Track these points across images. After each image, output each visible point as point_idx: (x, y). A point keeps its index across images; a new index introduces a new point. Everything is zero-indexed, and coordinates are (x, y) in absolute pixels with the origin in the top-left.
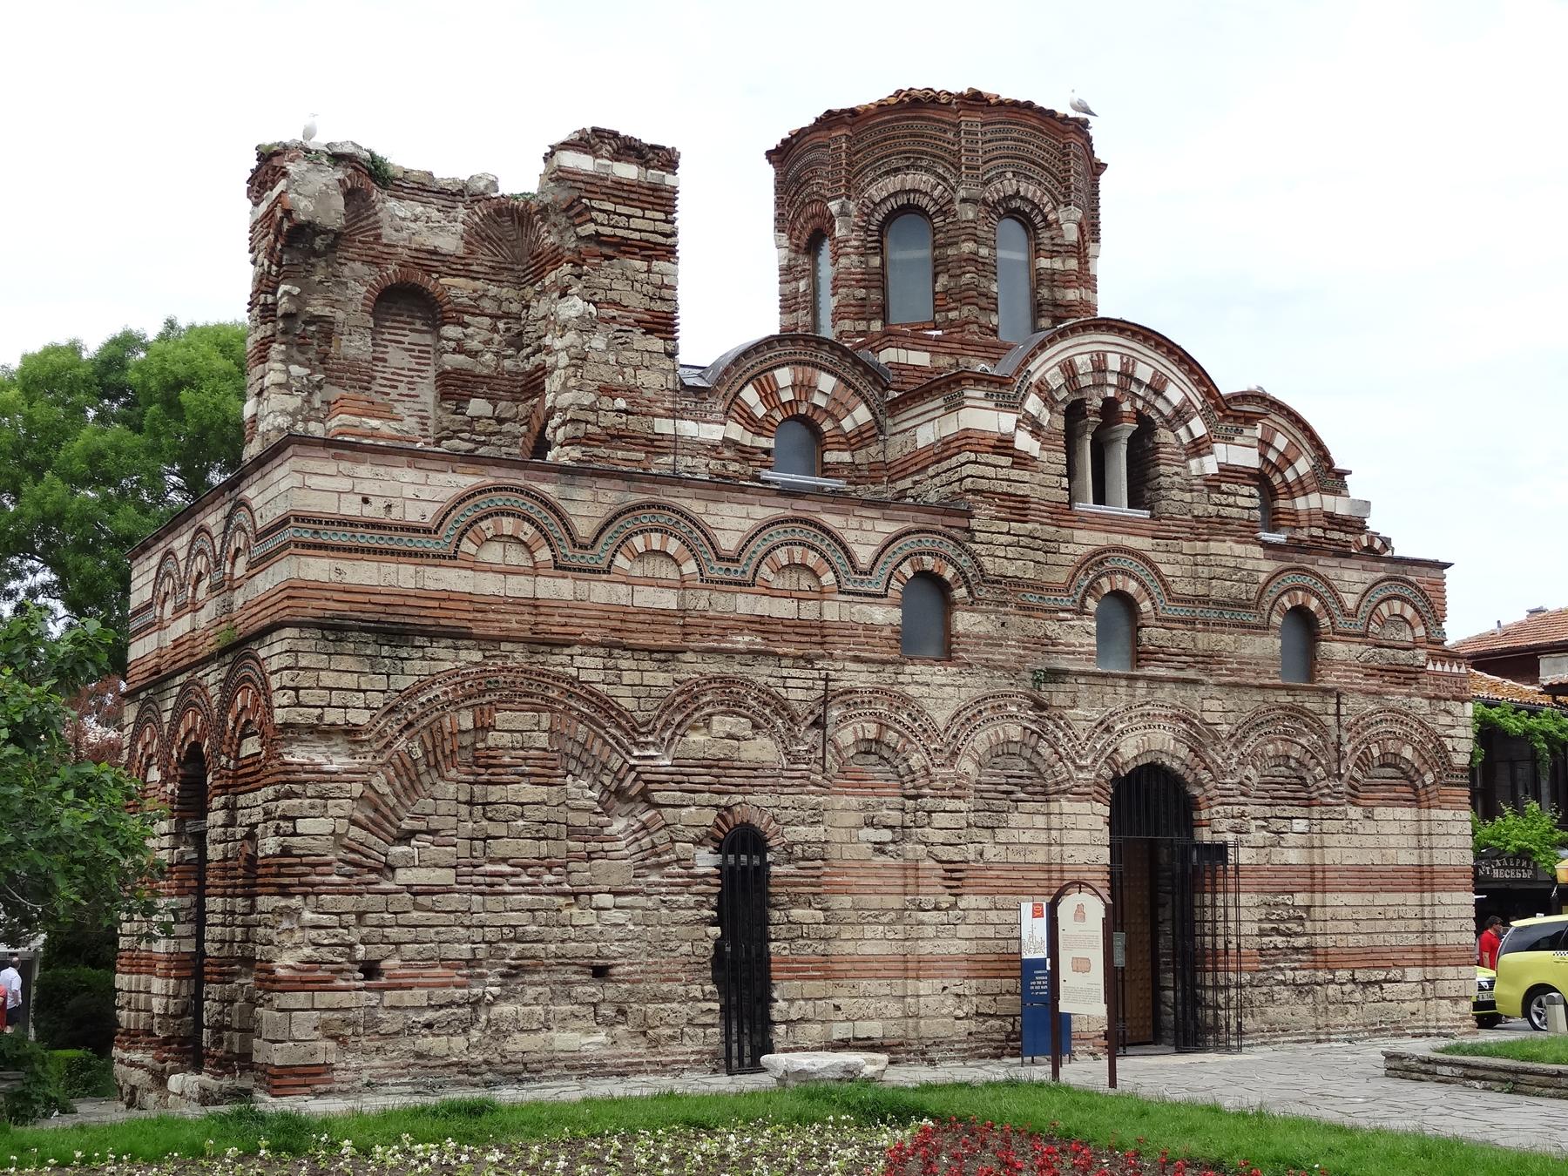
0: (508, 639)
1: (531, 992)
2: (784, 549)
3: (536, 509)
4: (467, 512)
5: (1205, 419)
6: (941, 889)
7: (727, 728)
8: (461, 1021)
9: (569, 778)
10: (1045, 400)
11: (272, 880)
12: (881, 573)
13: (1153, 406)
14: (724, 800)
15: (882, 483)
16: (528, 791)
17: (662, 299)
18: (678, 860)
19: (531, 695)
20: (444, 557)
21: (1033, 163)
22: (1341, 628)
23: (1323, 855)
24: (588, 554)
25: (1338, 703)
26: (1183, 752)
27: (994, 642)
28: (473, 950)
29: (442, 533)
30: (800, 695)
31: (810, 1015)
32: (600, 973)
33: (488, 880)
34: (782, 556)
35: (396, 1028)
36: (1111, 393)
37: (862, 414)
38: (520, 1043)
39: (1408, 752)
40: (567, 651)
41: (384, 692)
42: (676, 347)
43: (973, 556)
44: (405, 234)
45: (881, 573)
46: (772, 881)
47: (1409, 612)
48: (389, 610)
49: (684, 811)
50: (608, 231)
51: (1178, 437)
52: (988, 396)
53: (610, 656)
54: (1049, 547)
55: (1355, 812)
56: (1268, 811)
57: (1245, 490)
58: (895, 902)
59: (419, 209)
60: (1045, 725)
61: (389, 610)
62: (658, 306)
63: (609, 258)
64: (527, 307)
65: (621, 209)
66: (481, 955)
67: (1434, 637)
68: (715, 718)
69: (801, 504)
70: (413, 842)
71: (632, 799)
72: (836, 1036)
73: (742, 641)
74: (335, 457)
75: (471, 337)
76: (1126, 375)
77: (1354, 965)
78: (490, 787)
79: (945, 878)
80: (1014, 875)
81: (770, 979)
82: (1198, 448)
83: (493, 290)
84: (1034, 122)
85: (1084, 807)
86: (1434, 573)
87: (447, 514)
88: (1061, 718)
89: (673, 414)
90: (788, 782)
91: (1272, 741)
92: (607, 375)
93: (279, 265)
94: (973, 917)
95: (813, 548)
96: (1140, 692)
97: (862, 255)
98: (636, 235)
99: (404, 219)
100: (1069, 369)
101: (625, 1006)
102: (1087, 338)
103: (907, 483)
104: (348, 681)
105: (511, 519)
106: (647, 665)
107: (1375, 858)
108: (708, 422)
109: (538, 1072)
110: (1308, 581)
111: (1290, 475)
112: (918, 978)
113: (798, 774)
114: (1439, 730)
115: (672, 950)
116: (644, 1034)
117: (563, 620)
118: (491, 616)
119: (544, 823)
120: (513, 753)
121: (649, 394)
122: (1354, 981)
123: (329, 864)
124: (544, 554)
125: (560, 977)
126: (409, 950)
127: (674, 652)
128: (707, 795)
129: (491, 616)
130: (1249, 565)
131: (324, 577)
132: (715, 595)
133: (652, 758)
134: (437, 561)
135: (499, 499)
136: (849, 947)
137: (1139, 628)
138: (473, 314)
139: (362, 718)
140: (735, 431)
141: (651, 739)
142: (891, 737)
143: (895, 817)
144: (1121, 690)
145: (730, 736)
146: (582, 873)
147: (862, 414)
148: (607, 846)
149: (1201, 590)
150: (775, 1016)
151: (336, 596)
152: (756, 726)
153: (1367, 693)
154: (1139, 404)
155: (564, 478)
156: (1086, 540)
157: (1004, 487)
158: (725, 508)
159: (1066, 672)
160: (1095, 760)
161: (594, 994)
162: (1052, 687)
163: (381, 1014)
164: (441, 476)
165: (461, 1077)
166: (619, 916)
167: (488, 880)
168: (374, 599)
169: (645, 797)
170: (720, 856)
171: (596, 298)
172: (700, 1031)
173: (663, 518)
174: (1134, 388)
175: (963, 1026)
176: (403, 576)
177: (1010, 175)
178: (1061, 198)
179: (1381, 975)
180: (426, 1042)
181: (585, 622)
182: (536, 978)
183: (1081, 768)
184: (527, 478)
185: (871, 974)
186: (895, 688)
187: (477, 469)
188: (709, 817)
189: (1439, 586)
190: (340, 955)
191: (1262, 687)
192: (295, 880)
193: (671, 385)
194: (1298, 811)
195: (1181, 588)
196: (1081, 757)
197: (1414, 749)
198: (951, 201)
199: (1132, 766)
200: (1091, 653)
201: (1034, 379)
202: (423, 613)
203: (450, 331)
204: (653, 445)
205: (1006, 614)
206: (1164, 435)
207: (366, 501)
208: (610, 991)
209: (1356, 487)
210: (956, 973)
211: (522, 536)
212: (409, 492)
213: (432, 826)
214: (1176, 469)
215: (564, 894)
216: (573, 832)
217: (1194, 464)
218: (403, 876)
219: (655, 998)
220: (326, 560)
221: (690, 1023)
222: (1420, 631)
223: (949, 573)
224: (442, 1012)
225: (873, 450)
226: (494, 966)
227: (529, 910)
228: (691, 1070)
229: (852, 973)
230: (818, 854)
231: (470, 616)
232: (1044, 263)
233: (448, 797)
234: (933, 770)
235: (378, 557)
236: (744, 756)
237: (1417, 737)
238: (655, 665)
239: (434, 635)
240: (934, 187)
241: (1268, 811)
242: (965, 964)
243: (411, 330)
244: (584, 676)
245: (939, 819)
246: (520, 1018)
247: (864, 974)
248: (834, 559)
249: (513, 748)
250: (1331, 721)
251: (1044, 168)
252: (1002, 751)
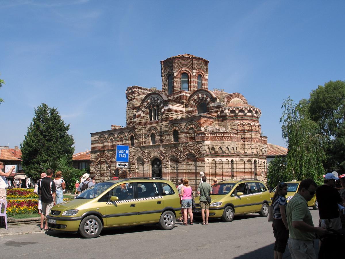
10: (145, 108)
27: (137, 143)
39: (193, 152)
57: (168, 113)
82: (163, 107)
95: (122, 135)
104: (94, 156)
107: (189, 171)
111: (207, 102)
139: (94, 159)
183: (147, 159)
196: (147, 158)
197: (195, 151)
250: (180, 148)
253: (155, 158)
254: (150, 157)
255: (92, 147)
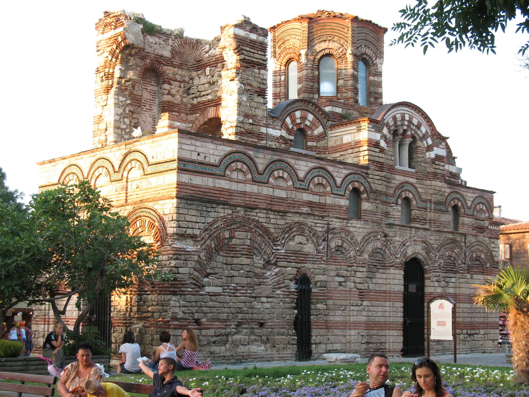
0: (240, 206)
1: (244, 331)
2: (317, 178)
3: (247, 160)
4: (227, 160)
5: (432, 139)
6: (358, 299)
7: (300, 240)
8: (224, 341)
9: (254, 256)
11: (167, 289)
12: (343, 188)
13: (417, 133)
14: (299, 265)
15: (326, 154)
16: (245, 260)
17: (263, 84)
18: (285, 287)
19: (244, 226)
20: (221, 176)
21: (370, 42)
22: (467, 212)
23: (459, 290)
24: (262, 177)
25: (465, 239)
26: (424, 254)
27: (373, 213)
28: (228, 316)
29: (221, 167)
30: (320, 229)
31: (322, 342)
32: (261, 325)
33: (232, 291)
34: (316, 180)
35: (205, 343)
36: (405, 128)
37: (320, 129)
38: (242, 349)
39: (483, 256)
40: (256, 211)
41: (203, 223)
42: (267, 101)
43: (369, 183)
44: (153, 49)
45: (343, 188)
46: (312, 294)
47: (484, 208)
48: (206, 194)
49: (288, 269)
50: (247, 58)
51: (423, 144)
52: (373, 127)
53: (267, 213)
54: (388, 180)
55: (469, 276)
56: (445, 275)
58: (344, 303)
59: (157, 40)
60: (387, 243)
61: (206, 194)
62: (262, 86)
63: (247, 68)
64: (192, 79)
65: (252, 50)
66: (230, 318)
67: (491, 217)
68: (297, 237)
69: (322, 162)
70: (210, 277)
71: (271, 264)
72: (328, 349)
73: (305, 210)
74: (190, 138)
75: (173, 89)
76: (410, 122)
77: (467, 328)
78: (234, 259)
79: (359, 295)
80: (378, 294)
81: (311, 328)
82: (430, 148)
83: (180, 72)
84: (371, 28)
85: (397, 271)
86: (491, 195)
87: (222, 160)
88: (392, 240)
89: (267, 126)
90: (316, 260)
91: (447, 251)
92: (247, 110)
93: (117, 58)
94: (366, 308)
95: (324, 178)
96: (413, 232)
97: (312, 70)
98: (256, 60)
99: (152, 43)
100: (394, 118)
101: (269, 337)
102: (400, 108)
103: (338, 155)
104: (194, 219)
105: (240, 163)
106: (278, 217)
108: (276, 129)
109: (246, 359)
110: (458, 196)
112: (350, 329)
113: (319, 257)
114: (491, 249)
115: (284, 318)
116: (275, 347)
117: (254, 200)
118: (233, 197)
119: (248, 271)
120: (240, 247)
121: (259, 118)
122: (467, 333)
123: (187, 284)
124: (249, 176)
125: (251, 326)
126: (209, 315)
127: (285, 212)
128: (294, 264)
129: (233, 197)
130: (443, 190)
131: (187, 182)
132: (297, 193)
133: (278, 250)
134: (219, 177)
135: (237, 156)
136: (331, 318)
137: (411, 210)
138: (174, 81)
139: (197, 232)
140: (284, 133)
141: (279, 243)
142: (345, 245)
143: (344, 273)
144: (408, 231)
145: (300, 243)
146: (258, 290)
147: (320, 129)
148: (265, 280)
149: (429, 198)
150: (312, 341)
151: (190, 188)
152: (307, 240)
153: (473, 235)
154: (413, 132)
155: (256, 149)
156: (399, 179)
157: (377, 159)
158: (301, 163)
159: (394, 225)
160: (401, 256)
161: (261, 333)
162: (389, 230)
163: (201, 338)
164: (221, 147)
165: (224, 361)
166: (268, 305)
167: (232, 291)
168: (201, 189)
169: (275, 264)
170: (297, 285)
171: (244, 82)
172: (291, 346)
173: (284, 165)
174: (412, 126)
175: (364, 346)
176: (208, 182)
177: (363, 46)
178: (378, 55)
179: (473, 332)
180: (214, 348)
181: (261, 201)
182: (245, 326)
183: (396, 258)
184: (245, 149)
185: (337, 327)
186: (347, 228)
187: (231, 144)
188: (294, 271)
189: (492, 199)
190: (191, 317)
191: (446, 232)
192: (178, 290)
193: (265, 115)
194: (453, 275)
195: (424, 197)
196: (397, 254)
198: (345, 54)
199: (410, 258)
200: (399, 218)
201: (385, 122)
202: (215, 195)
203: (166, 86)
204: (260, 136)
205: (378, 203)
206: (419, 143)
207: (199, 154)
208: (265, 331)
209: (459, 163)
210: (362, 328)
211: (243, 169)
212: (211, 152)
213: (216, 272)
214: (423, 155)
215: (253, 297)
216: (257, 276)
217: (428, 154)
218: (208, 289)
219: (278, 334)
220: (187, 175)
221: (288, 344)
222: (487, 215)
223: (362, 189)
224: (218, 338)
225: (324, 142)
226: (234, 322)
227: (245, 303)
228: (289, 360)
229: (332, 327)
230: (324, 285)
231: (229, 197)
232: (371, 78)
233: (221, 261)
234: (357, 257)
235: (202, 175)
236: (305, 250)
237: (485, 251)
238: (280, 217)
239: (218, 204)
240: (339, 49)
241: (445, 275)
242: (364, 325)
243: (151, 85)
244: (261, 220)
245: (358, 274)
246: (242, 340)
247: (336, 327)
248: (331, 182)
249: (240, 245)
250: (463, 244)
251: (373, 44)
252: (375, 252)
253: (413, 257)
254: (406, 252)
255: (180, 185)
